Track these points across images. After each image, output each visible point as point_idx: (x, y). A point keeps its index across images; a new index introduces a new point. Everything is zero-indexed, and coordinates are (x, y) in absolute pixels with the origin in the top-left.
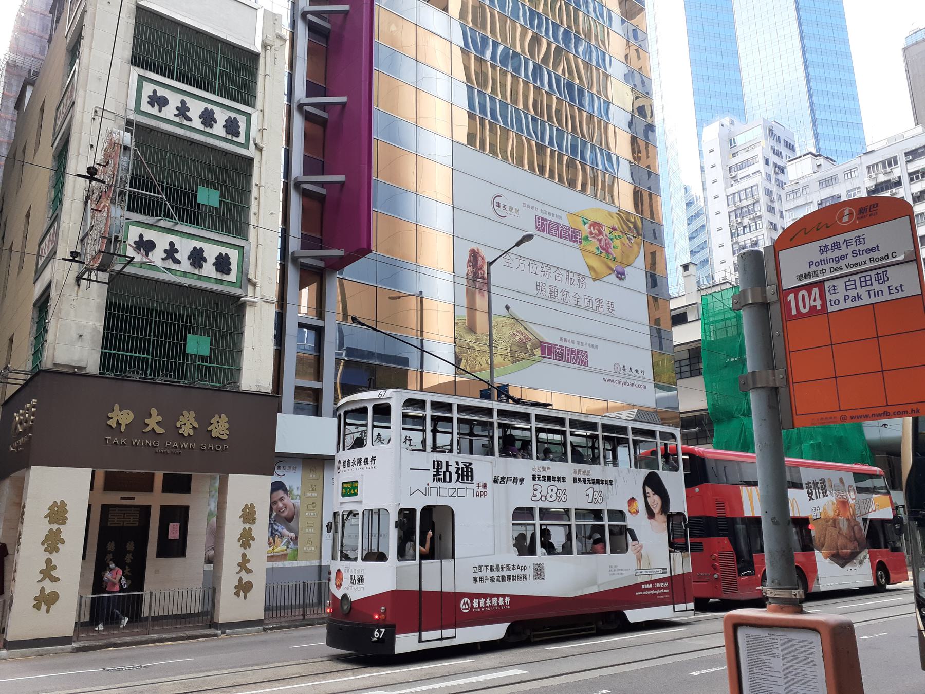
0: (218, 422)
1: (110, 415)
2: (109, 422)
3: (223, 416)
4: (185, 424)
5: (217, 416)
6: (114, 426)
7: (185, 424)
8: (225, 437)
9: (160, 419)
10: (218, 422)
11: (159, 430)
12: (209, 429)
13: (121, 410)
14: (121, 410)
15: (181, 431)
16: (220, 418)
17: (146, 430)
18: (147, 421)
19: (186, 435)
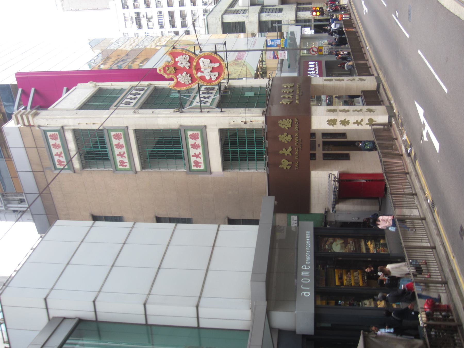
0: (283, 125)
1: (285, 168)
2: (289, 168)
3: (279, 122)
4: (286, 139)
5: (280, 125)
6: (290, 167)
7: (286, 139)
8: (291, 121)
9: (284, 149)
10: (283, 125)
11: (290, 149)
12: (287, 129)
13: (282, 164)
14: (282, 164)
15: (290, 141)
16: (280, 124)
17: (291, 155)
18: (286, 155)
19: (291, 138)
